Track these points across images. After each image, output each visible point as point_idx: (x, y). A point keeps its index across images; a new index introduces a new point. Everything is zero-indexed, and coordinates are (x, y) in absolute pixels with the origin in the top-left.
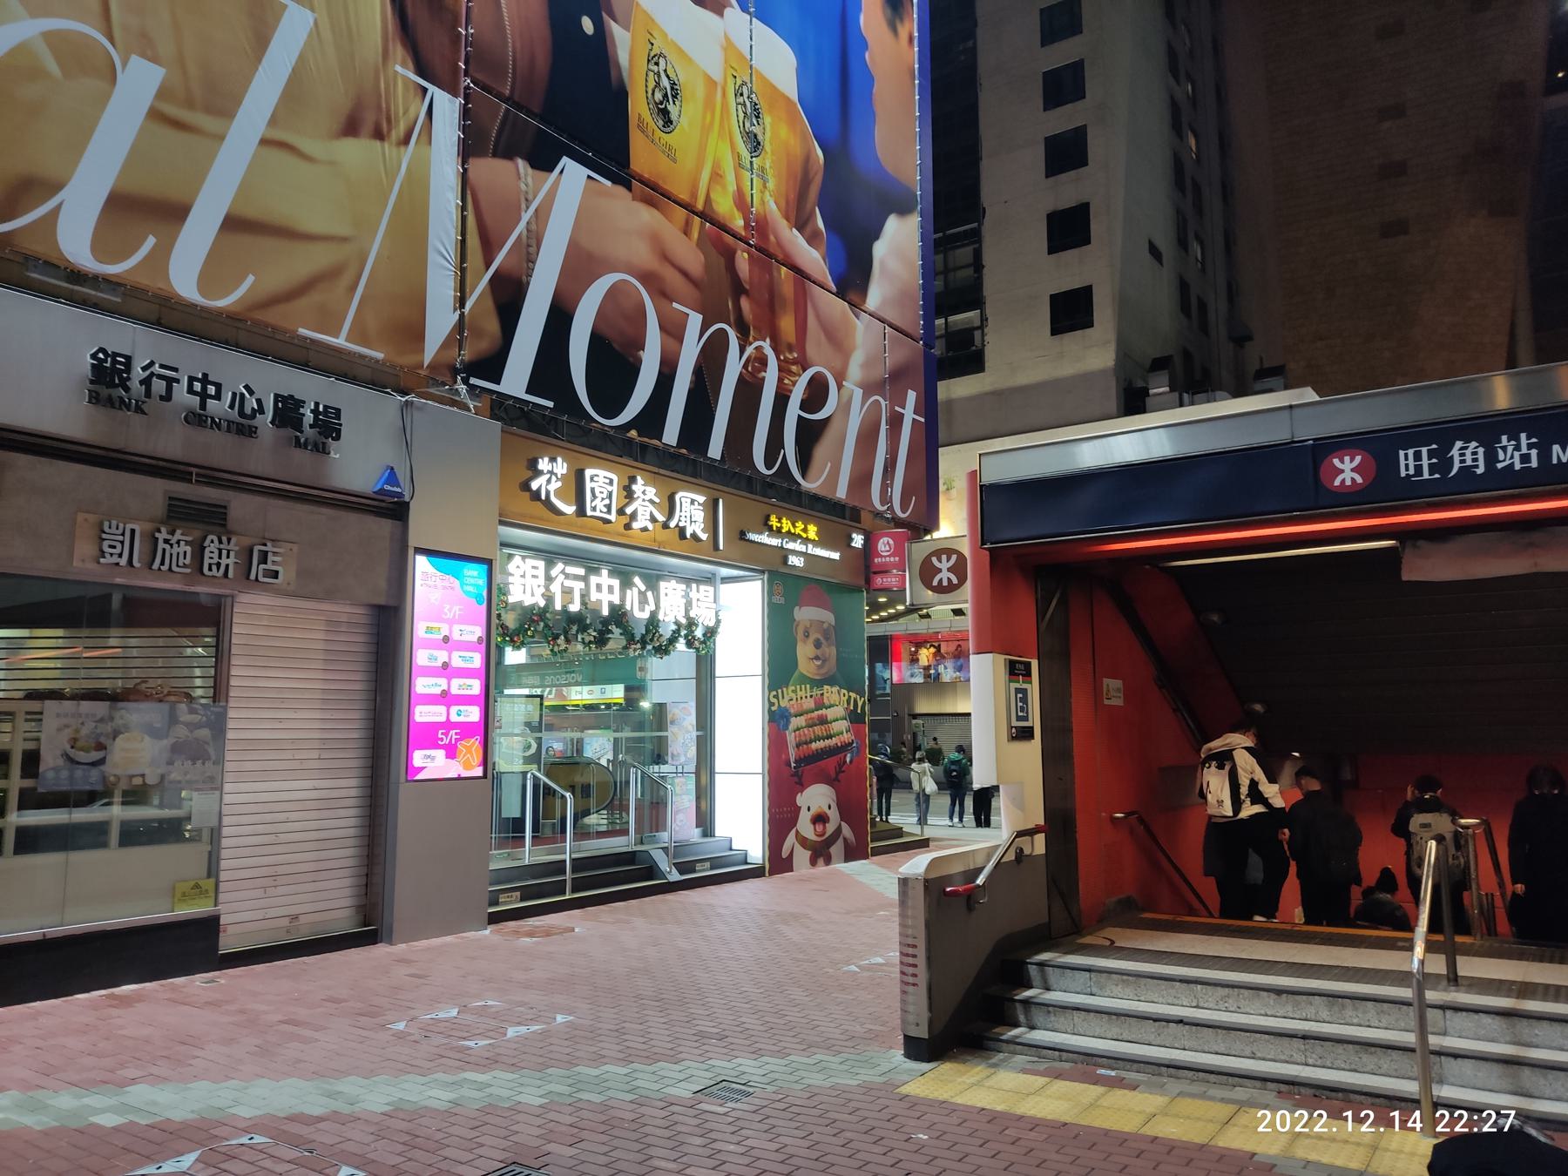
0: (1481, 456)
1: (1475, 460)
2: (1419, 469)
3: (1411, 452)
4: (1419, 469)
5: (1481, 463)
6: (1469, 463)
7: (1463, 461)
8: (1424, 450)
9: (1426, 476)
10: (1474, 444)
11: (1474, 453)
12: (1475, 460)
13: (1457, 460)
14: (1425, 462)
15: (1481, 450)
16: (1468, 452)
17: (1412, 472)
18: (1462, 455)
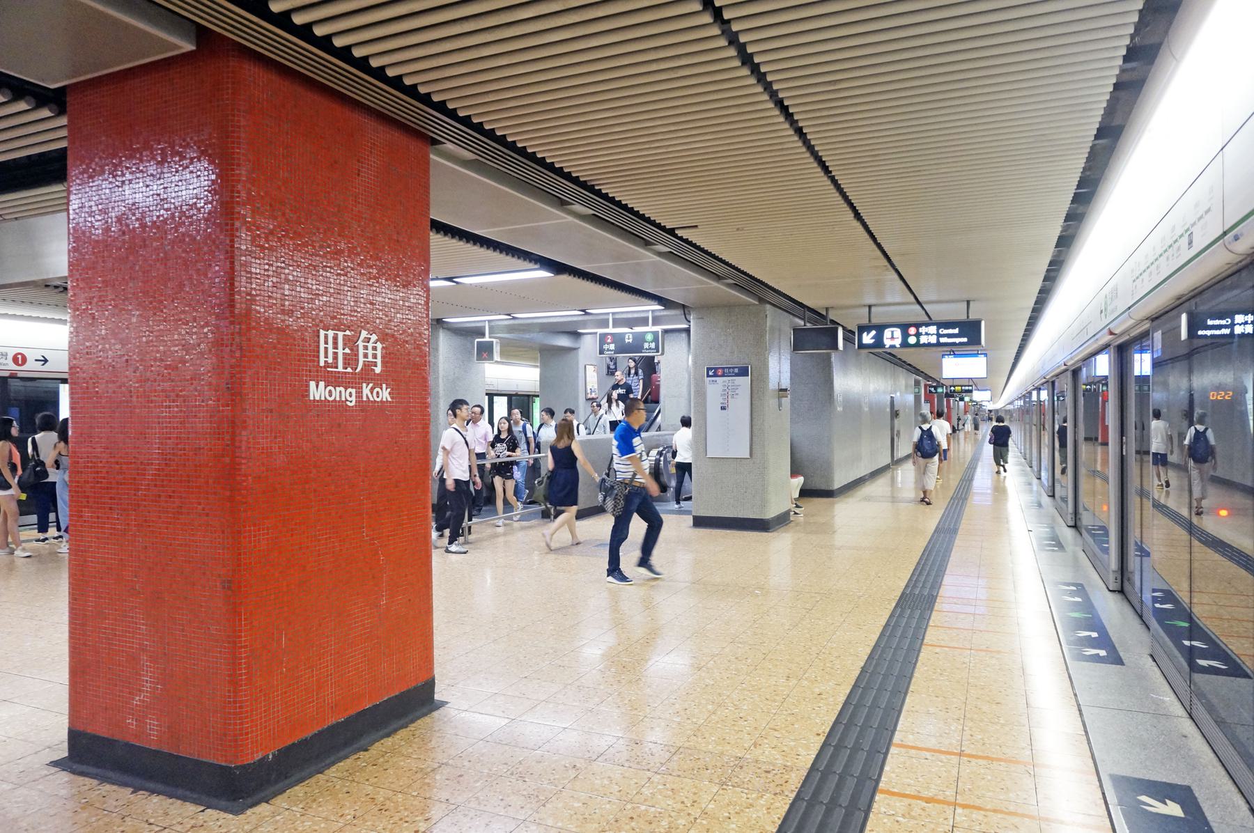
0: (379, 353)
1: (375, 356)
2: (335, 354)
3: (331, 333)
4: (335, 354)
5: (379, 360)
6: (370, 359)
7: (366, 356)
8: (341, 334)
9: (340, 369)
10: (374, 337)
11: (375, 348)
12: (375, 356)
13: (361, 351)
14: (340, 351)
15: (379, 345)
16: (370, 345)
17: (330, 360)
18: (366, 348)
